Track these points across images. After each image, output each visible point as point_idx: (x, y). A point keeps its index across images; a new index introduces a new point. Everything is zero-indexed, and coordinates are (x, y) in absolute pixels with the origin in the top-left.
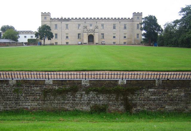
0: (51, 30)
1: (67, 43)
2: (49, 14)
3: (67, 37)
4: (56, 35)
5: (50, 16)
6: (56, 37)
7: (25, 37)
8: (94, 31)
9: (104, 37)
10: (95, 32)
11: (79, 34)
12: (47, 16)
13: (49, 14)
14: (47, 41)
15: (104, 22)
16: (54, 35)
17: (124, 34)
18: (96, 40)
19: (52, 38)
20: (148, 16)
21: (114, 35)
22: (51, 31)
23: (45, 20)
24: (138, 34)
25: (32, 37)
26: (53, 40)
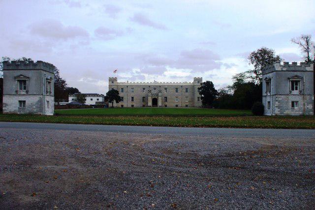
1: (133, 106)
3: (133, 100)
7: (92, 99)
8: (157, 95)
14: (115, 104)
18: (160, 103)
24: (198, 98)
25: (98, 99)
26: (120, 104)
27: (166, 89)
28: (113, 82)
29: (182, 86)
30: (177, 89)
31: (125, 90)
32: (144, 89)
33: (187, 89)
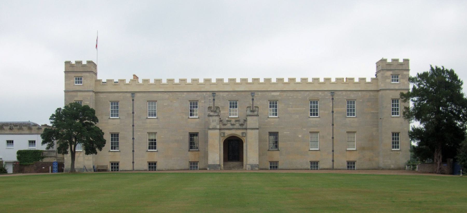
0: (96, 120)
1: (152, 165)
2: (91, 68)
3: (153, 144)
4: (115, 136)
5: (96, 74)
6: (115, 146)
8: (243, 125)
9: (280, 145)
10: (246, 129)
11: (192, 135)
12: (84, 74)
13: (91, 68)
14: (84, 160)
15: (278, 94)
16: (107, 137)
17: (348, 132)
18: (251, 155)
19: (101, 149)
20: (428, 70)
21: (314, 135)
22: (98, 125)
23: (78, 88)
24: (395, 135)
25: (32, 142)
26: (105, 156)
27: (273, 104)
28: (79, 80)
29: (333, 93)
30: (314, 102)
31: (125, 107)
32: (194, 104)
33: (351, 102)
